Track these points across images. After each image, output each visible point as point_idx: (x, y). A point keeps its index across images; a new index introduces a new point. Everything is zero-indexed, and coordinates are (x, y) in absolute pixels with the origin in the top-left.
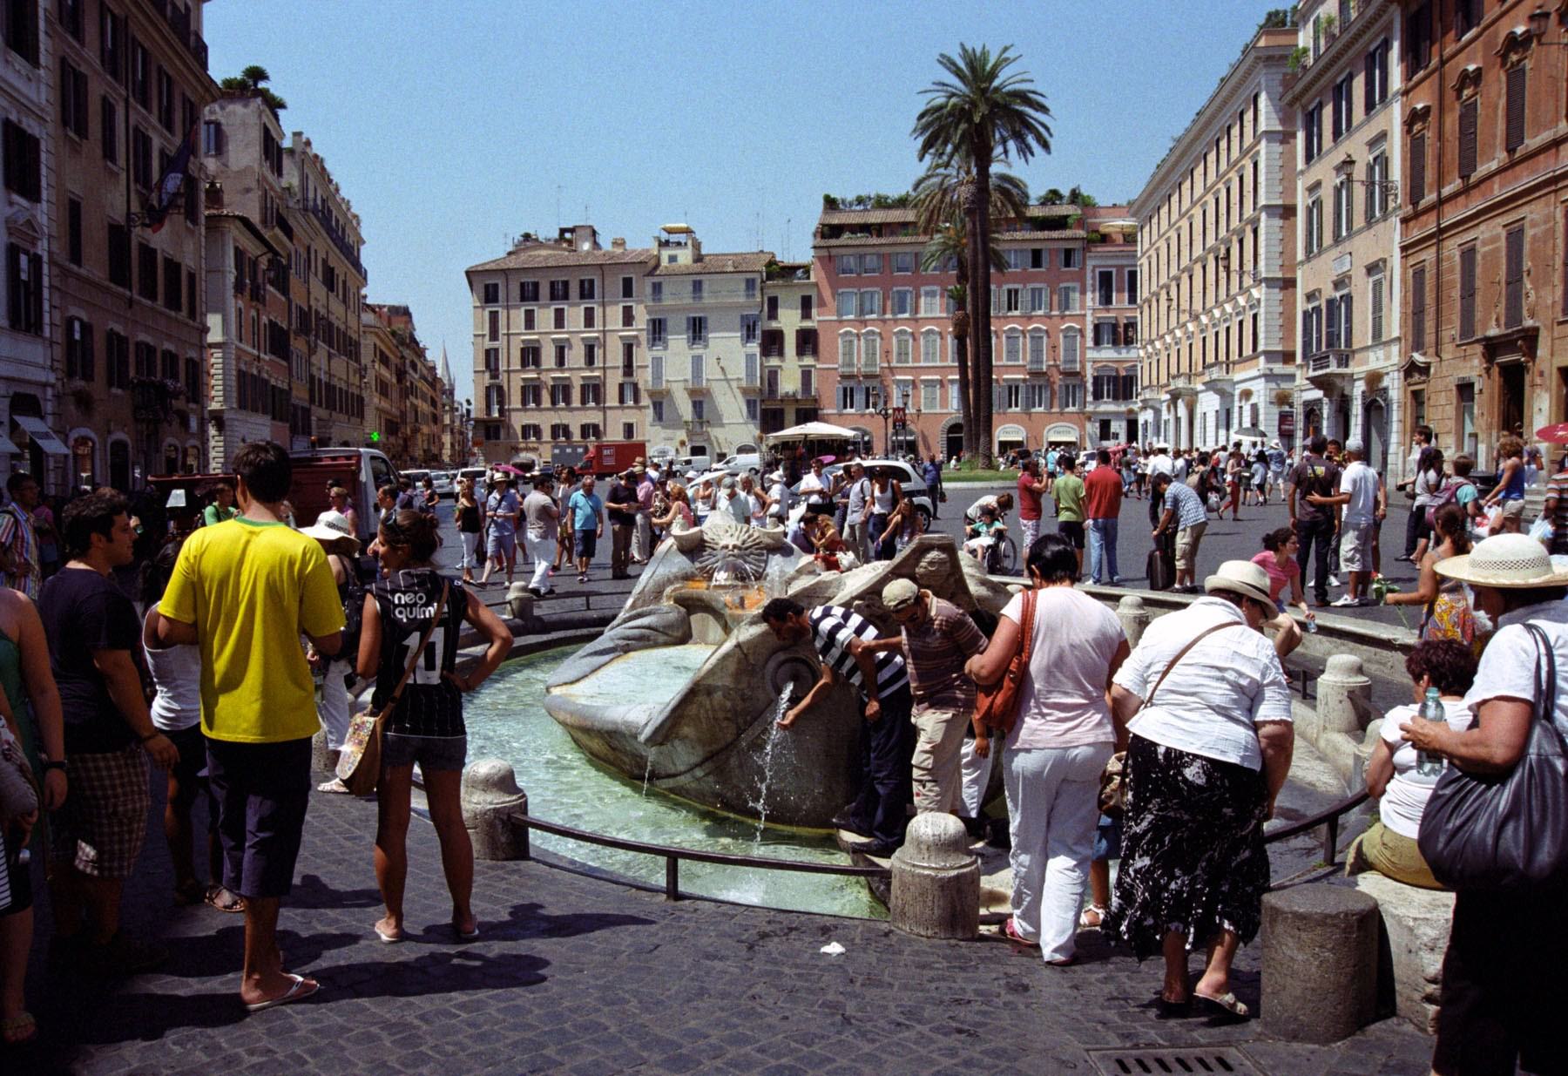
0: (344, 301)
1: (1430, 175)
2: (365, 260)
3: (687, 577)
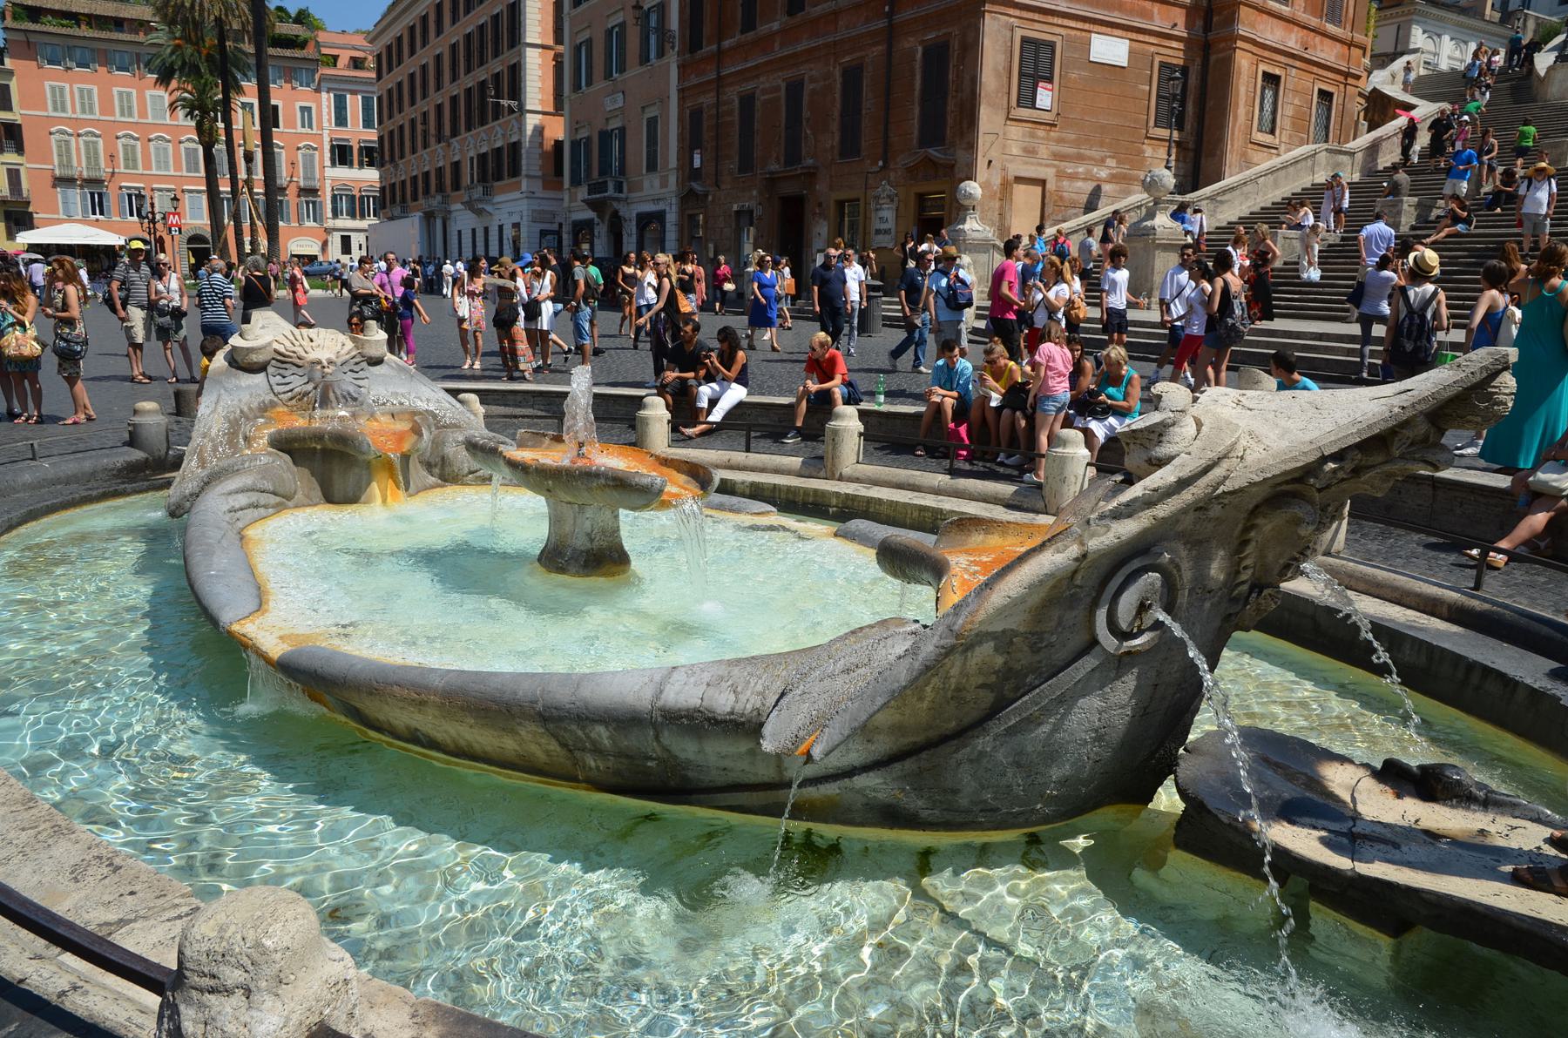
1: (707, 30)
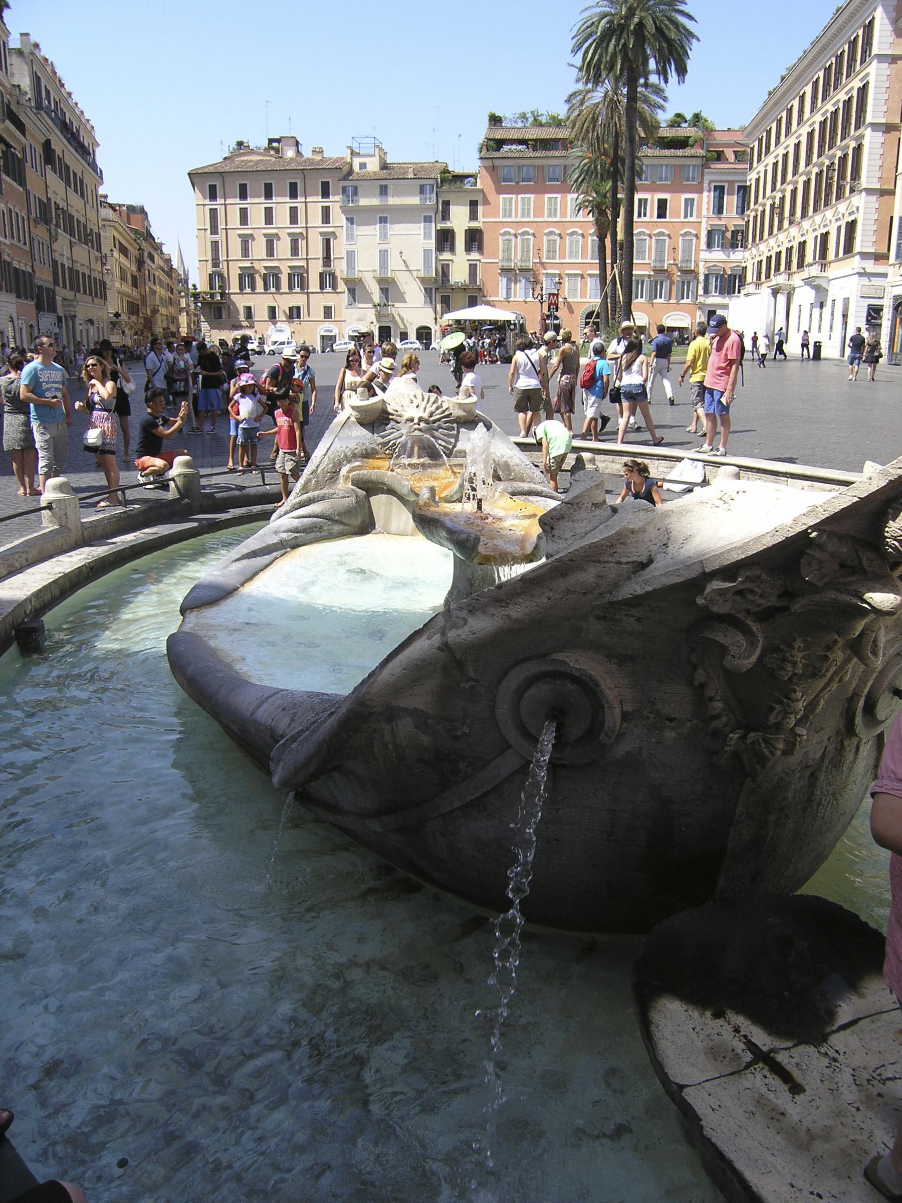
0: (82, 196)
2: (100, 163)
3: (368, 455)
